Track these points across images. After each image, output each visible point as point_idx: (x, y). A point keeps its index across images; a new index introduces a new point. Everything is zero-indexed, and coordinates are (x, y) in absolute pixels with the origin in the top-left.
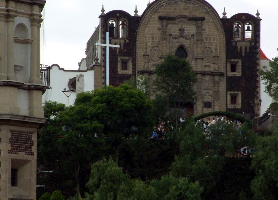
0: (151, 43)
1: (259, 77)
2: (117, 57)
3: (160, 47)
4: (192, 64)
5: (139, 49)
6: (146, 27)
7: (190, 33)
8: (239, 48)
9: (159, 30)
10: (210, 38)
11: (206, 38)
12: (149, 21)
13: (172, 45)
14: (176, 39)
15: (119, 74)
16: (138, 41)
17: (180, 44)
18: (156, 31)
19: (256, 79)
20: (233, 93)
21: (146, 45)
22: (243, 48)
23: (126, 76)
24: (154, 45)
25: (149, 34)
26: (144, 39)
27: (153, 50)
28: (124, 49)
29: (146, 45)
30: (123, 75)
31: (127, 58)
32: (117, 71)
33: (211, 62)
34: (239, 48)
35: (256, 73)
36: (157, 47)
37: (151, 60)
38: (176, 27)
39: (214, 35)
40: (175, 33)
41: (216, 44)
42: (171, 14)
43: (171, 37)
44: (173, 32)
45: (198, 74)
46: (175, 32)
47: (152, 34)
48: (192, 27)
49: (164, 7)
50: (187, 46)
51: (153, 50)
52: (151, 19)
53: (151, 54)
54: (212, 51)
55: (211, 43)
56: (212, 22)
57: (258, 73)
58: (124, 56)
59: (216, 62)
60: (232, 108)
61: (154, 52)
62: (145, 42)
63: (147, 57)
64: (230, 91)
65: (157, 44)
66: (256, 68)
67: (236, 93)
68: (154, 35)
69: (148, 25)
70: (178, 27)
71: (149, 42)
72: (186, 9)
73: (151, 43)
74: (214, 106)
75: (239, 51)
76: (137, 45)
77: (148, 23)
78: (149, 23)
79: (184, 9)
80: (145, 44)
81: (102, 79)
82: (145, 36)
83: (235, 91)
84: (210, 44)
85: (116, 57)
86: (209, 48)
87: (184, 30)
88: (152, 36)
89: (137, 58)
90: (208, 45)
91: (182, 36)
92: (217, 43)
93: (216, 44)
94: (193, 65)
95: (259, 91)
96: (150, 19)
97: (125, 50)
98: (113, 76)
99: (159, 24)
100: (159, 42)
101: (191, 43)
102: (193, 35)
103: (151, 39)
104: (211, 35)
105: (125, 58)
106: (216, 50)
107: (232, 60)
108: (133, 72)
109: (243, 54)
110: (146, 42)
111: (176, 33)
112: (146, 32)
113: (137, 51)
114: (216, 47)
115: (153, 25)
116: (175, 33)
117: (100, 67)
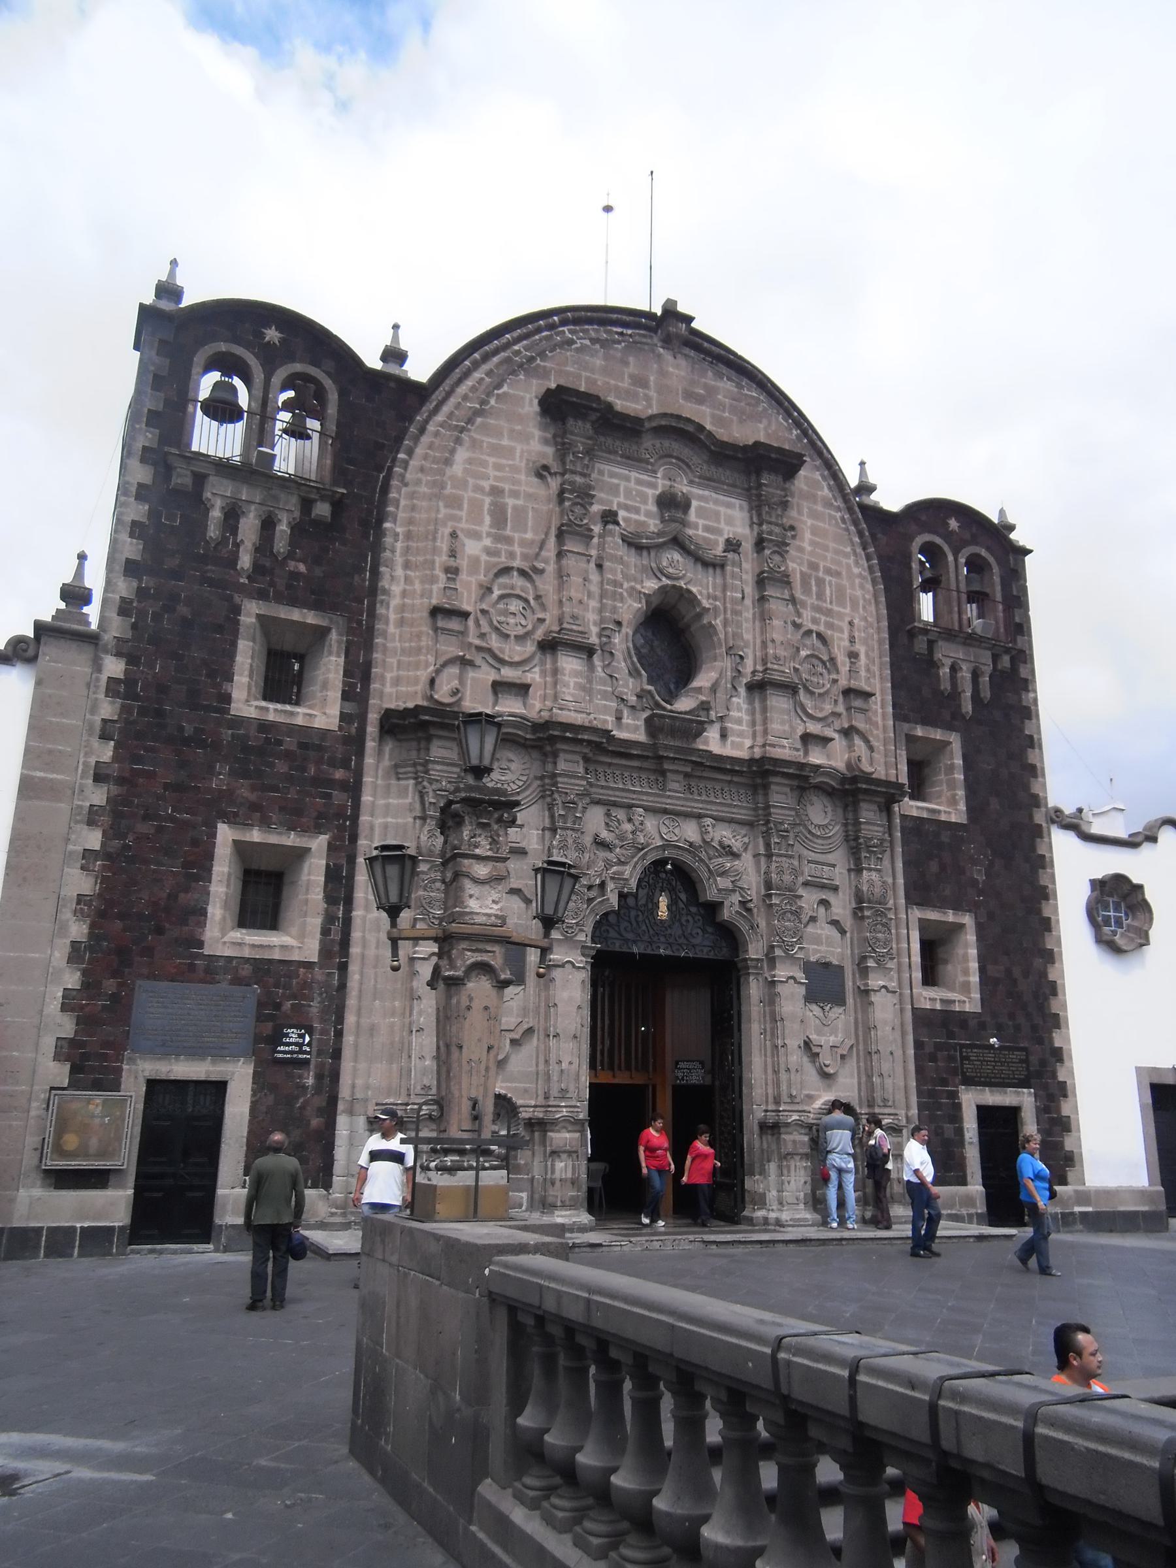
0: (487, 542)
1: (1046, 840)
2: (237, 598)
3: (547, 585)
4: (734, 714)
5: (399, 572)
6: (458, 441)
7: (718, 532)
8: (945, 671)
9: (540, 476)
10: (820, 582)
11: (805, 579)
12: (478, 413)
13: (619, 577)
14: (639, 548)
15: (239, 722)
16: (395, 522)
17: (665, 581)
18: (523, 477)
19: (1033, 848)
20: (933, 915)
21: (453, 554)
22: (965, 674)
23: (290, 743)
24: (503, 560)
25: (478, 489)
26: (443, 511)
27: (497, 593)
28: (291, 556)
29: (453, 554)
30: (265, 727)
31: (311, 618)
32: (227, 699)
33: (831, 719)
34: (945, 671)
35: (1031, 817)
36: (522, 573)
37: (479, 649)
38: (639, 482)
39: (838, 574)
40: (634, 516)
41: (851, 623)
42: (618, 402)
43: (610, 527)
44: (627, 508)
45: (777, 773)
46: (637, 511)
47: (496, 492)
48: (729, 506)
49: (577, 350)
50: (706, 604)
51: (497, 593)
52: (493, 402)
53: (483, 612)
54: (832, 660)
55: (828, 613)
56: (827, 504)
57: (1039, 818)
58: (294, 602)
59: (860, 724)
60: (938, 1007)
61: (501, 606)
62: (448, 531)
63: (454, 624)
64: (923, 903)
65: (525, 557)
66: (1027, 787)
67: (950, 917)
68: (510, 502)
69: (472, 434)
70: (653, 486)
71: (476, 536)
72: (700, 400)
73: (487, 542)
74: (865, 993)
75: (946, 685)
76: (388, 540)
77: (470, 421)
78: (479, 420)
79: (689, 395)
80: (444, 545)
81: (95, 743)
82: (448, 490)
83: (942, 905)
84: (823, 618)
85: (230, 599)
86: (820, 636)
87: (685, 506)
88: (492, 504)
89: (379, 626)
90: (815, 621)
91: (678, 543)
92: (856, 621)
93: (851, 623)
94: (739, 721)
95: (1053, 918)
96: (483, 402)
97: (302, 568)
98: (189, 730)
99: (546, 442)
100: (542, 545)
101: (724, 588)
102: (733, 546)
103: (487, 520)
104: (828, 571)
105: (296, 615)
106: (853, 655)
107: (919, 732)
108: (343, 717)
109: (967, 707)
110: (454, 535)
111: (642, 518)
112: (457, 468)
113: (384, 583)
114: (852, 640)
115: (505, 442)
116: (634, 516)
117: (89, 649)
